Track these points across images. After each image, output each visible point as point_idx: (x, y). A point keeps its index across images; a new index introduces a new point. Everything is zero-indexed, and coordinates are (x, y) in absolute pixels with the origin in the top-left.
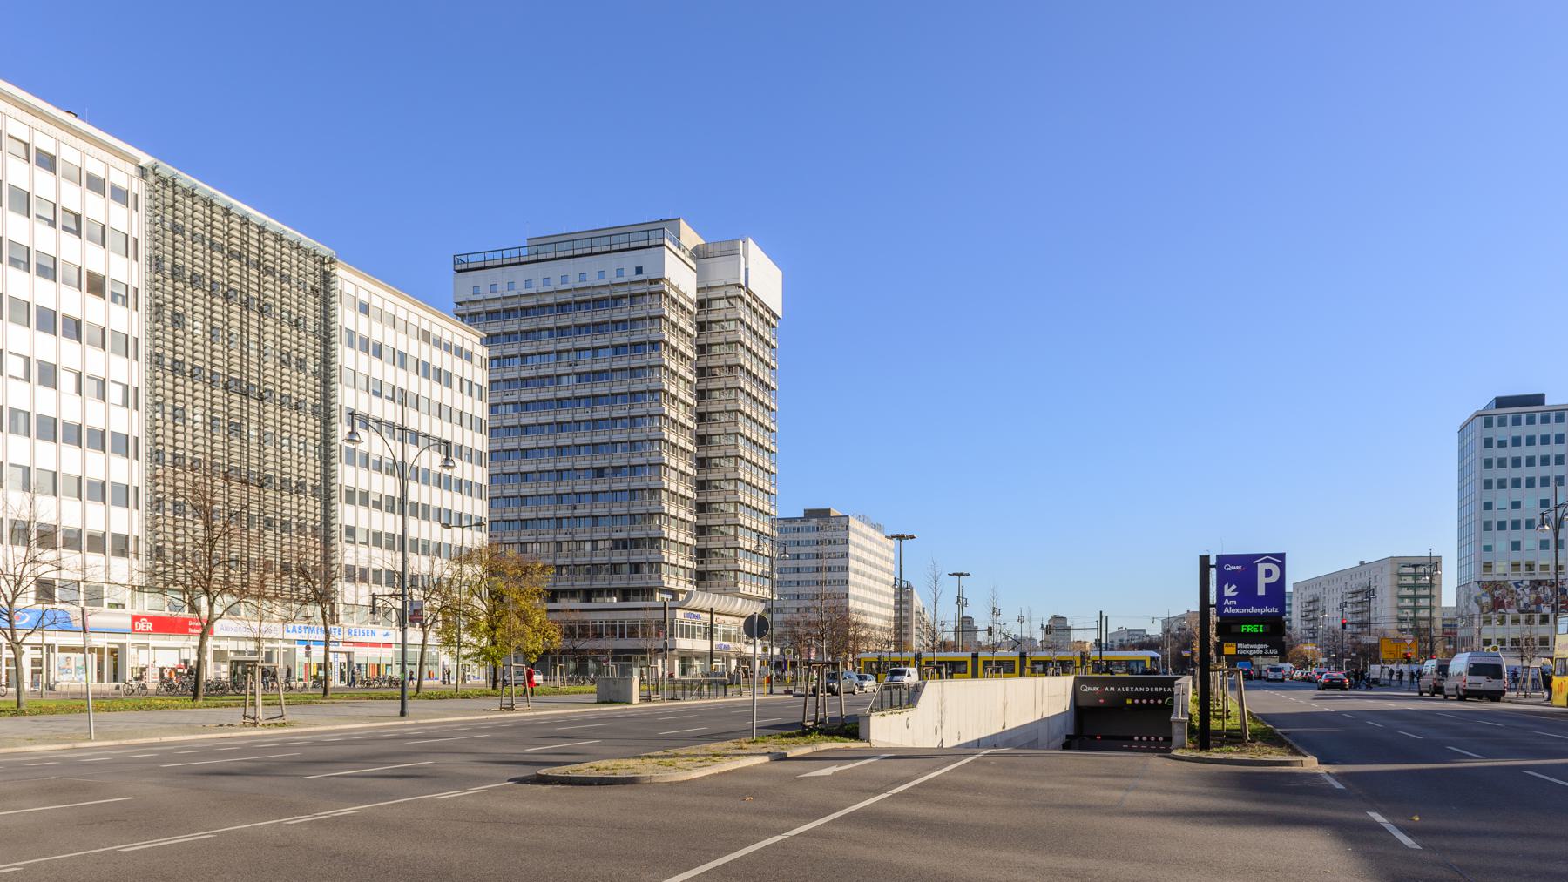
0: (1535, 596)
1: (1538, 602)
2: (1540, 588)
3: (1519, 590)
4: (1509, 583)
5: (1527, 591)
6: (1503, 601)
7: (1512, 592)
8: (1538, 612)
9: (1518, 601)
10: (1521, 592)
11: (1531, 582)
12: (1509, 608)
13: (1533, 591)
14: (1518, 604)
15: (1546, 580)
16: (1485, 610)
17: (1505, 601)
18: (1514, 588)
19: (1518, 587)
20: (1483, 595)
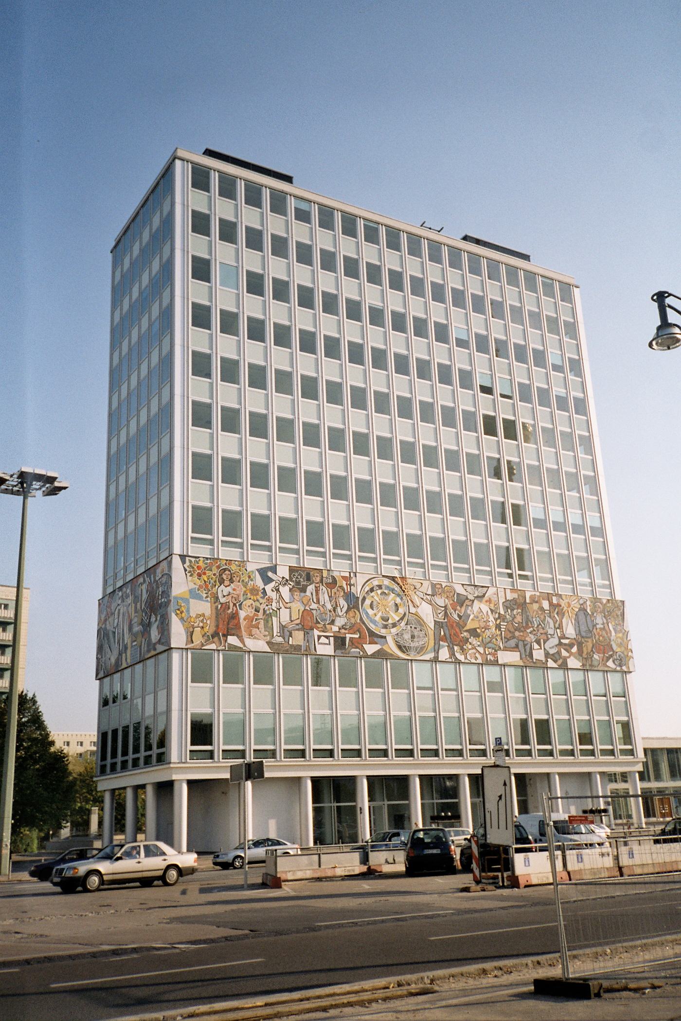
2: (311, 588)
3: (269, 588)
5: (285, 591)
6: (235, 616)
7: (254, 591)
9: (268, 617)
10: (273, 595)
12: (251, 635)
13: (297, 594)
14: (269, 628)
16: (198, 639)
17: (242, 614)
18: (259, 582)
19: (267, 580)
20: (194, 595)
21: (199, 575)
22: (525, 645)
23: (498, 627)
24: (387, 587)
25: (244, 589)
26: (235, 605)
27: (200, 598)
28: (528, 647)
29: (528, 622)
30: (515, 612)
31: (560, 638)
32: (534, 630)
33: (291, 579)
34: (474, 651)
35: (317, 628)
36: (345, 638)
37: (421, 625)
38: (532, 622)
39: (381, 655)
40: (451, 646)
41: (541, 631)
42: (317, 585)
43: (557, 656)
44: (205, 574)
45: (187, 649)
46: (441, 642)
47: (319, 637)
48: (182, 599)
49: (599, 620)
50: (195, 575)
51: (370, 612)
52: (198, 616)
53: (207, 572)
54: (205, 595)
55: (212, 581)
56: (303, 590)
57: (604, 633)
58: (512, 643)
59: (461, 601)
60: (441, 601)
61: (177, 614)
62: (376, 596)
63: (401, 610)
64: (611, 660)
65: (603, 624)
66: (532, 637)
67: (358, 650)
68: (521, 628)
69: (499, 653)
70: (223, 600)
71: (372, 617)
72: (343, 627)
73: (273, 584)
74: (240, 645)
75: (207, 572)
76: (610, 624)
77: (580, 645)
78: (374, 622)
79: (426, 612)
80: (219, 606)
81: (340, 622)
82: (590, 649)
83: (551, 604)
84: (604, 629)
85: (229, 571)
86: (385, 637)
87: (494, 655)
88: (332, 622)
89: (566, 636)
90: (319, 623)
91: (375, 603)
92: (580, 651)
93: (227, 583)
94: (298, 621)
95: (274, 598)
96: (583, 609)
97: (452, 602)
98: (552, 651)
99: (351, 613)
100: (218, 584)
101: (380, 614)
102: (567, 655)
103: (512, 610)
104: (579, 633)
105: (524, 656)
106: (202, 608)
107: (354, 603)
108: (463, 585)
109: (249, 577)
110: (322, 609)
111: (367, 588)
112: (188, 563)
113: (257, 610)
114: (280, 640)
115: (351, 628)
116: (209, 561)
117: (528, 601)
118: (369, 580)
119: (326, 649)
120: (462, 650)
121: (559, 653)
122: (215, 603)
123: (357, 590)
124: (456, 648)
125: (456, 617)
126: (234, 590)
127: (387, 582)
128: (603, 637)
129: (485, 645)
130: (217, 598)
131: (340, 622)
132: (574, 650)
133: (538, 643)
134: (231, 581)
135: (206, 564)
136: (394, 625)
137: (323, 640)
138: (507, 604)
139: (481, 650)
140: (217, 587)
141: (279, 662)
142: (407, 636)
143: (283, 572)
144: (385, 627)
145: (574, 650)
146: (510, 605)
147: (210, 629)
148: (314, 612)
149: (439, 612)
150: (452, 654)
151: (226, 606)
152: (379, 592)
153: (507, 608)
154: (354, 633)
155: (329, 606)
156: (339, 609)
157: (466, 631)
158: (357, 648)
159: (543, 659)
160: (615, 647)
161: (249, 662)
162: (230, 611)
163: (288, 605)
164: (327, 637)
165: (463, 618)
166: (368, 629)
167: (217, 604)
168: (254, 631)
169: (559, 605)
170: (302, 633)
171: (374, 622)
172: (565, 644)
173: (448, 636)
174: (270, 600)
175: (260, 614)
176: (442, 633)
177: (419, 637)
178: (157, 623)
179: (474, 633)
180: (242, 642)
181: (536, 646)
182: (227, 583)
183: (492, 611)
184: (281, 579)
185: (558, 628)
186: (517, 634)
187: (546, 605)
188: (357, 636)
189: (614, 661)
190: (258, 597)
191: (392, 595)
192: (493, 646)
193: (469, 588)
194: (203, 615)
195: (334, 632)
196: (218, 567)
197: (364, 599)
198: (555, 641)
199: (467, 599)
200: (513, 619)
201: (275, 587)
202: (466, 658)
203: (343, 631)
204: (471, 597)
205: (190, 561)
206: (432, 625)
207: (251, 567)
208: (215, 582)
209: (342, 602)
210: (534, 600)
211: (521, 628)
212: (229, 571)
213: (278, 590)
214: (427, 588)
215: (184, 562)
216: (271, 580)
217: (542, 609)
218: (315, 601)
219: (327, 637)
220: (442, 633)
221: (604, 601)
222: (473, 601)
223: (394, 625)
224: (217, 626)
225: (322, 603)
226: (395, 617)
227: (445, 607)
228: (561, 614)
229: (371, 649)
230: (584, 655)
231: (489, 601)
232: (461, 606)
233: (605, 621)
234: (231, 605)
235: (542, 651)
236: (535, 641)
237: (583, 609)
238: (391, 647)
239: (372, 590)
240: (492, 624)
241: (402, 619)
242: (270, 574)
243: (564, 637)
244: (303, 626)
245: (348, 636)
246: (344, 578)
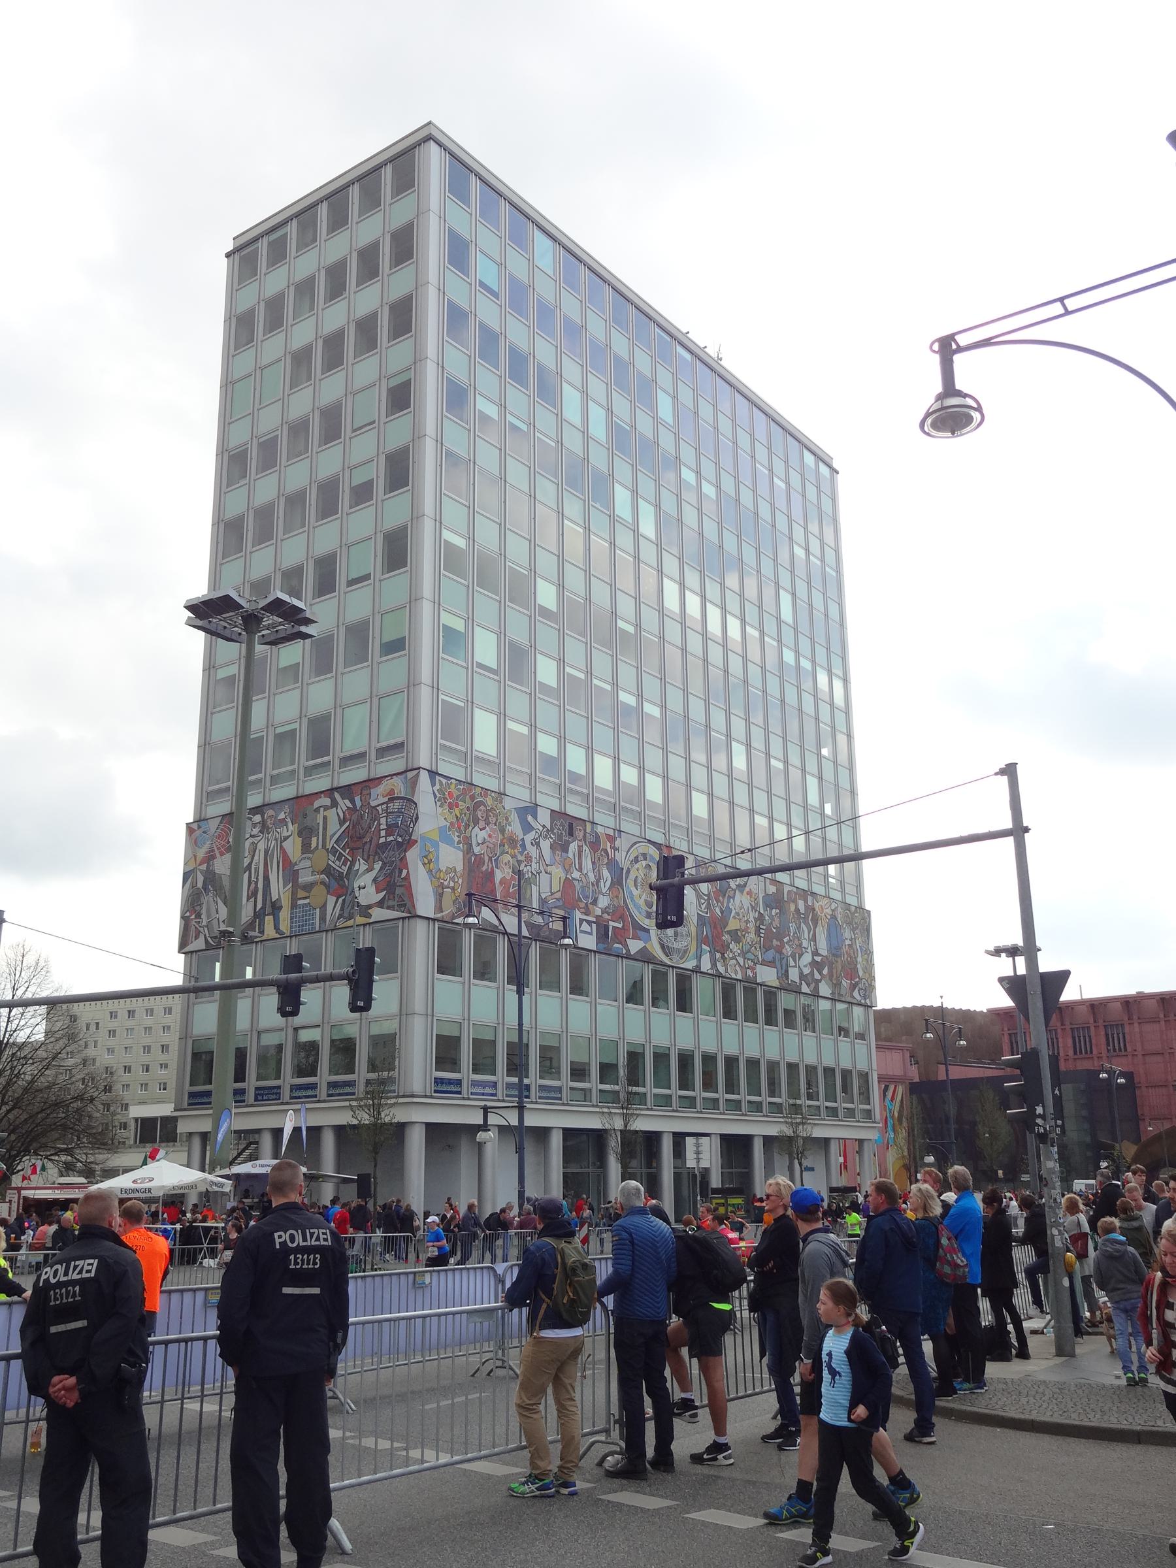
2: (573, 847)
3: (529, 838)
5: (545, 845)
7: (513, 842)
16: (448, 909)
17: (498, 875)
18: (515, 828)
19: (528, 828)
21: (451, 807)
25: (501, 837)
26: (490, 859)
27: (449, 842)
28: (784, 961)
32: (790, 940)
34: (734, 961)
40: (713, 951)
41: (796, 942)
42: (580, 844)
43: (809, 977)
44: (457, 806)
45: (434, 920)
46: (704, 946)
48: (431, 840)
49: (847, 934)
50: (446, 806)
51: (635, 892)
52: (447, 872)
53: (460, 803)
54: (456, 839)
55: (465, 819)
58: (770, 954)
61: (424, 864)
64: (857, 990)
67: (620, 946)
72: (604, 911)
73: (532, 835)
75: (460, 803)
80: (473, 859)
81: (603, 902)
82: (839, 972)
83: (807, 907)
85: (485, 806)
87: (753, 969)
88: (595, 902)
89: (820, 952)
90: (581, 901)
91: (639, 879)
93: (482, 824)
94: (558, 895)
95: (534, 856)
96: (834, 917)
97: (714, 889)
100: (472, 825)
101: (644, 897)
105: (780, 975)
106: (451, 858)
109: (507, 819)
110: (584, 880)
112: (437, 787)
115: (613, 914)
116: (462, 787)
118: (632, 846)
121: (812, 973)
122: (467, 854)
125: (718, 910)
126: (490, 836)
128: (849, 955)
129: (744, 954)
130: (471, 845)
131: (603, 902)
135: (458, 790)
137: (585, 927)
139: (741, 960)
140: (471, 828)
145: (825, 972)
148: (576, 883)
149: (703, 901)
150: (714, 965)
151: (479, 859)
152: (644, 863)
153: (767, 906)
155: (592, 878)
156: (602, 881)
157: (729, 932)
158: (621, 943)
159: (797, 980)
162: (484, 868)
163: (549, 869)
164: (589, 923)
165: (726, 912)
166: (632, 916)
167: (469, 856)
173: (710, 936)
174: (529, 859)
176: (705, 933)
177: (682, 935)
178: (373, 874)
179: (736, 936)
181: (792, 963)
182: (482, 824)
184: (541, 828)
188: (620, 926)
190: (516, 850)
192: (753, 957)
194: (455, 871)
195: (597, 917)
196: (472, 798)
197: (628, 871)
198: (807, 958)
201: (535, 839)
203: (606, 916)
205: (441, 782)
207: (509, 804)
208: (469, 818)
209: (606, 874)
212: (485, 806)
213: (538, 844)
215: (433, 784)
217: (797, 910)
218: (577, 867)
219: (589, 923)
220: (705, 933)
221: (853, 909)
227: (708, 895)
228: (815, 921)
229: (634, 946)
231: (750, 893)
234: (486, 859)
237: (834, 917)
239: (636, 860)
240: (751, 926)
242: (530, 818)
243: (816, 953)
244: (564, 903)
245: (611, 924)
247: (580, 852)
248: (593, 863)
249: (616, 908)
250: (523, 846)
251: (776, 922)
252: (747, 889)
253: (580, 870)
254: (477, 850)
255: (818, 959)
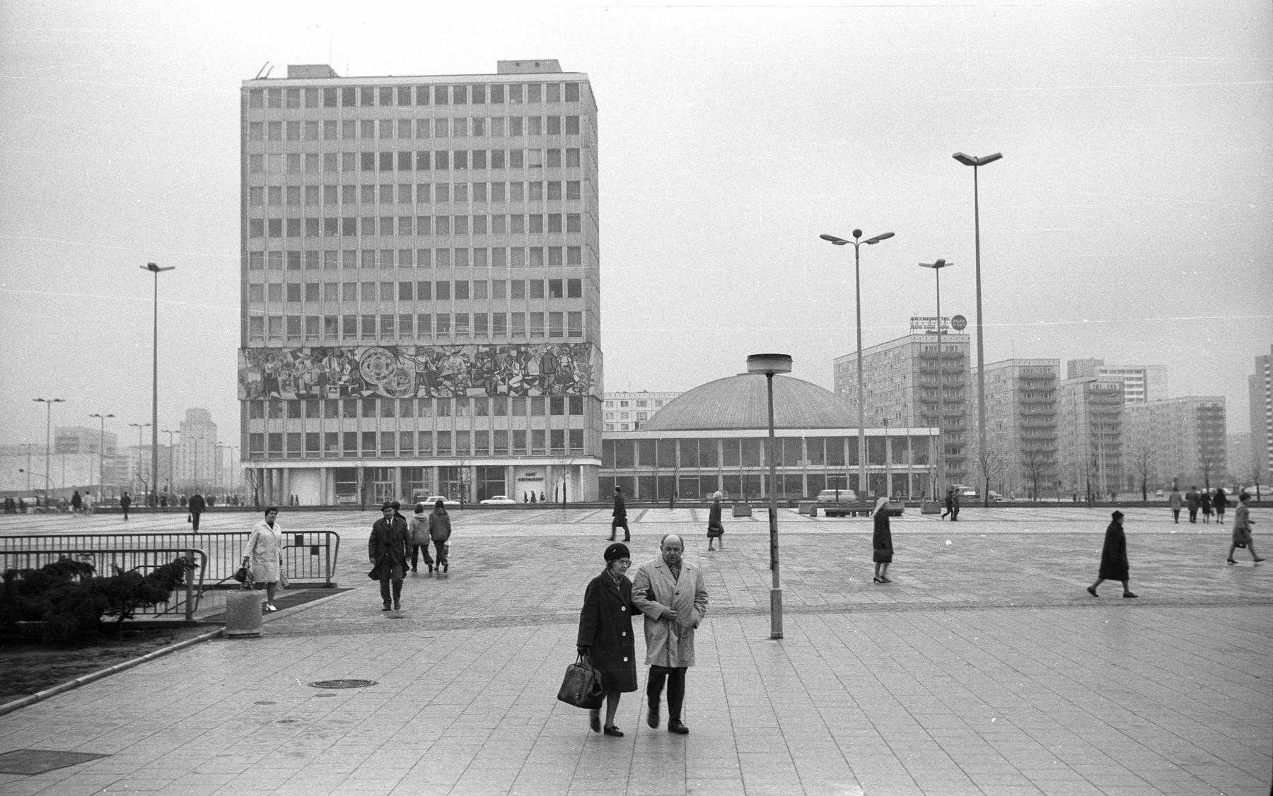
0: (318, 371)
1: (322, 380)
2: (326, 360)
3: (297, 362)
4: (285, 351)
5: (308, 363)
6: (277, 378)
7: (288, 365)
8: (322, 397)
9: (296, 379)
11: (313, 349)
12: (285, 390)
14: (297, 387)
15: (332, 348)
17: (280, 379)
18: (290, 359)
19: (296, 357)
20: (251, 370)
22: (491, 383)
23: (469, 372)
24: (380, 353)
27: (255, 372)
28: (493, 385)
29: (496, 366)
30: (485, 361)
31: (523, 376)
33: (312, 355)
35: (329, 383)
36: (347, 388)
37: (405, 376)
38: (500, 369)
39: (375, 396)
41: (507, 372)
47: (330, 389)
49: (564, 360)
56: (321, 361)
57: (568, 369)
58: (481, 382)
59: (440, 357)
60: (422, 359)
62: (373, 361)
63: (390, 368)
65: (568, 362)
66: (499, 377)
68: (490, 371)
69: (468, 390)
70: (268, 371)
71: (368, 374)
74: (278, 396)
76: (575, 363)
77: (542, 380)
78: (370, 377)
79: (409, 365)
83: (519, 353)
84: (568, 366)
86: (377, 386)
88: (340, 379)
92: (542, 384)
96: (549, 353)
98: (515, 386)
99: (353, 372)
102: (529, 387)
103: (483, 359)
104: (542, 371)
107: (356, 367)
108: (442, 346)
111: (366, 355)
112: (247, 353)
113: (290, 376)
114: (305, 392)
117: (498, 352)
119: (334, 395)
120: (437, 389)
123: (357, 358)
124: (432, 389)
125: (435, 369)
127: (380, 350)
128: (565, 371)
131: (345, 378)
132: (537, 382)
133: (503, 380)
134: (274, 360)
136: (385, 377)
137: (332, 390)
138: (480, 356)
139: (453, 388)
141: (303, 404)
142: (394, 384)
143: (307, 352)
144: (378, 379)
145: (537, 382)
146: (480, 356)
147: (260, 388)
150: (428, 393)
151: (270, 375)
154: (355, 384)
155: (338, 369)
160: (576, 378)
161: (285, 405)
168: (287, 388)
169: (526, 352)
170: (318, 387)
171: (370, 377)
172: (528, 380)
174: (298, 369)
175: (292, 378)
179: (447, 378)
180: (279, 393)
181: (501, 383)
183: (465, 362)
185: (524, 369)
186: (485, 375)
187: (514, 353)
189: (573, 389)
191: (383, 358)
193: (446, 348)
197: (363, 362)
198: (520, 378)
199: (445, 355)
200: (483, 366)
202: (439, 394)
204: (448, 354)
206: (412, 374)
209: (348, 367)
210: (502, 351)
211: (490, 371)
213: (303, 363)
214: (412, 351)
216: (299, 357)
219: (336, 388)
221: (572, 346)
222: (449, 356)
223: (385, 377)
224: (265, 387)
225: (333, 368)
226: (385, 372)
227: (426, 363)
228: (528, 359)
229: (365, 393)
230: (546, 387)
232: (439, 361)
233: (570, 360)
235: (506, 387)
236: (501, 380)
238: (382, 392)
239: (370, 356)
241: (391, 373)
243: (528, 375)
246: (350, 351)
247: (330, 360)
248: (339, 364)
249: (353, 380)
250: (294, 365)
251: (489, 365)
252: (461, 353)
253: (330, 367)
254: (268, 371)
255: (530, 378)
